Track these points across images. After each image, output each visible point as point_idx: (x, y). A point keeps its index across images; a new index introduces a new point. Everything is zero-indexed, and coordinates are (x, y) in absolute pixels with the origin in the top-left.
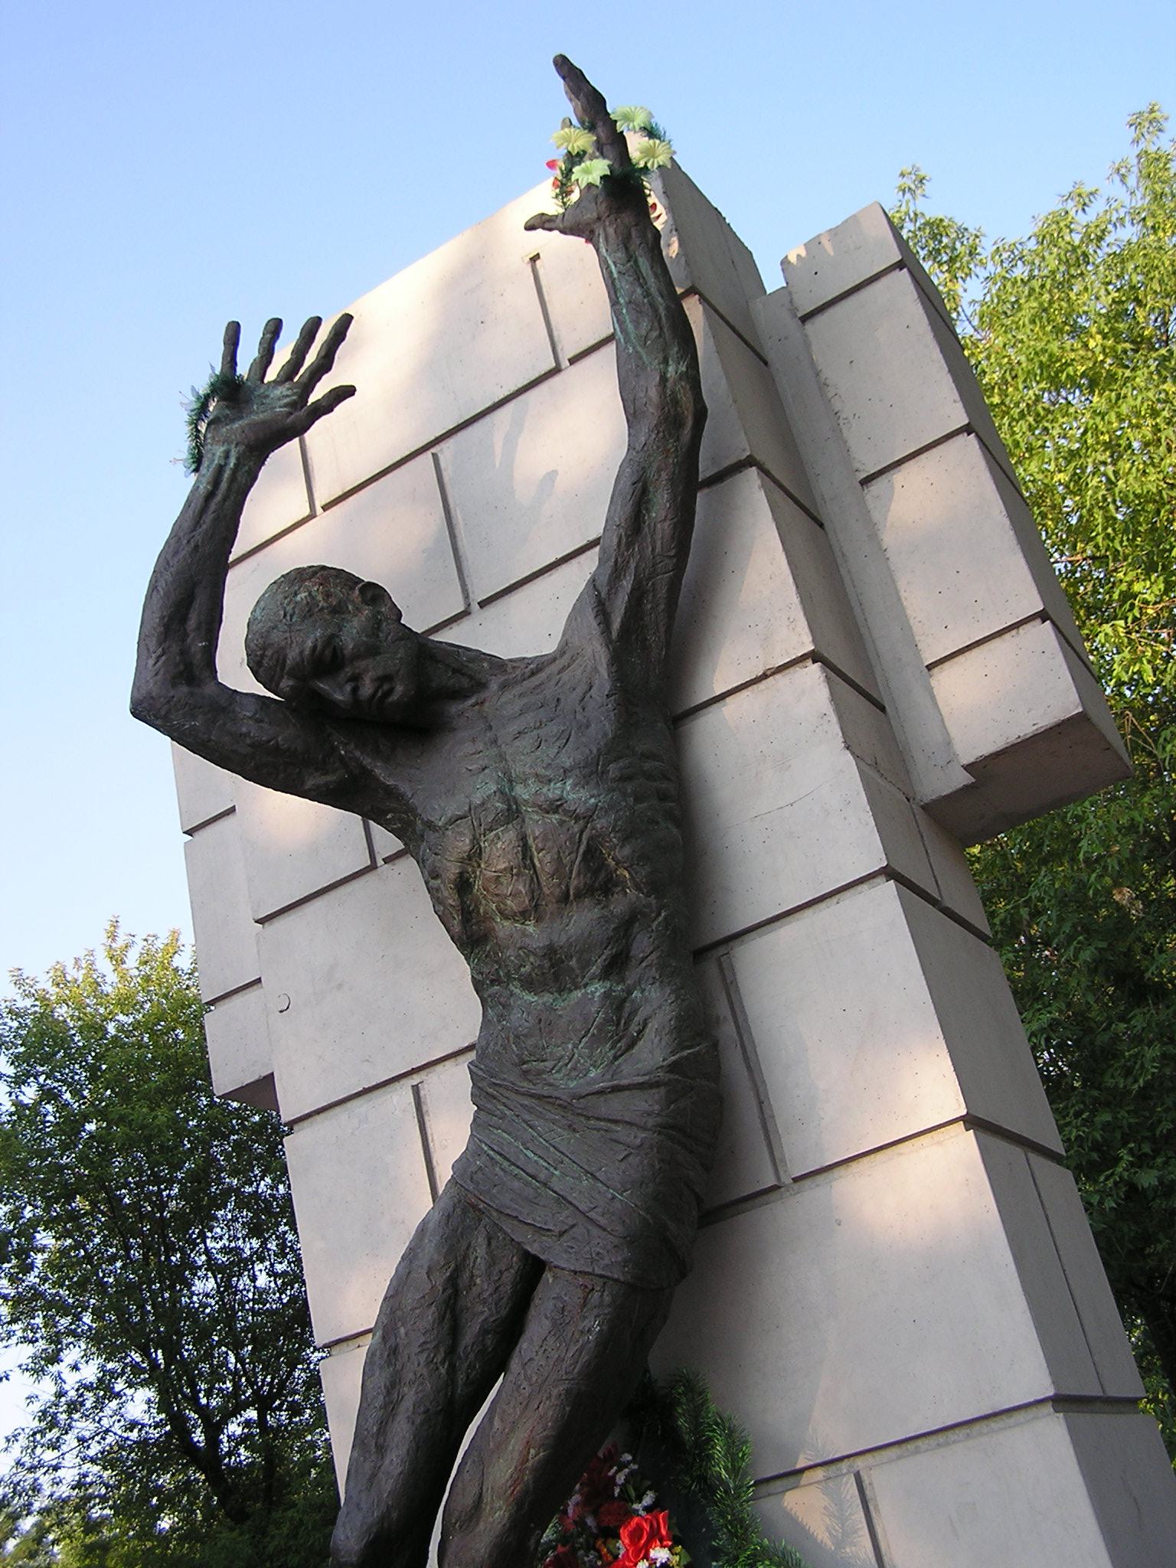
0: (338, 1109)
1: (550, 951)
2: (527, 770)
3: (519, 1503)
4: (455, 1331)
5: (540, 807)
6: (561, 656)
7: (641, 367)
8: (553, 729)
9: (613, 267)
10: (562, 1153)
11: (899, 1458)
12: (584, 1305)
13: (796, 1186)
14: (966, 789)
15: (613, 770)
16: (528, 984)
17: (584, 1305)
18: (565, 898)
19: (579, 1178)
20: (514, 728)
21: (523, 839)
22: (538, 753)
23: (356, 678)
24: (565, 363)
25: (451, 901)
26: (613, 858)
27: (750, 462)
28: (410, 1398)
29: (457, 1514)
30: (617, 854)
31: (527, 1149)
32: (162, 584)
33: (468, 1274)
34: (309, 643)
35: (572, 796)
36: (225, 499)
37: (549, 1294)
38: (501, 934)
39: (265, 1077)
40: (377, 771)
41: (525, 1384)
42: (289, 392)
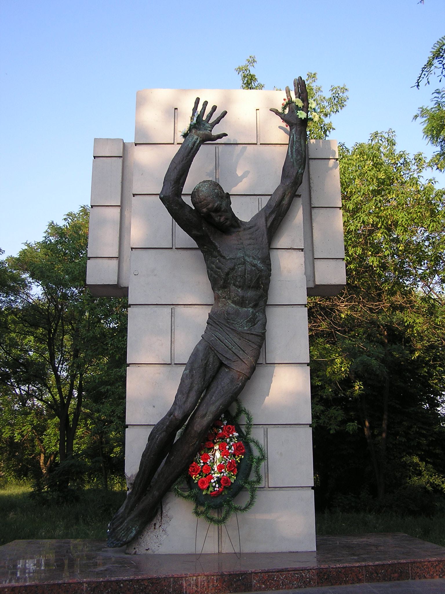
0: (146, 306)
1: (243, 297)
2: (251, 254)
4: (205, 376)
5: (252, 265)
6: (255, 226)
7: (293, 166)
9: (295, 138)
10: (236, 343)
11: (274, 427)
12: (238, 379)
13: (266, 365)
14: (311, 288)
16: (234, 302)
17: (238, 379)
18: (249, 287)
19: (240, 351)
20: (248, 242)
21: (245, 269)
22: (253, 251)
23: (221, 216)
24: (259, 143)
25: (223, 277)
26: (261, 282)
28: (196, 388)
29: (200, 415)
31: (226, 340)
32: (178, 168)
33: (208, 363)
34: (216, 204)
35: (259, 265)
36: (195, 151)
38: (232, 289)
39: (105, 285)
40: (211, 237)
41: (222, 392)
42: (210, 127)
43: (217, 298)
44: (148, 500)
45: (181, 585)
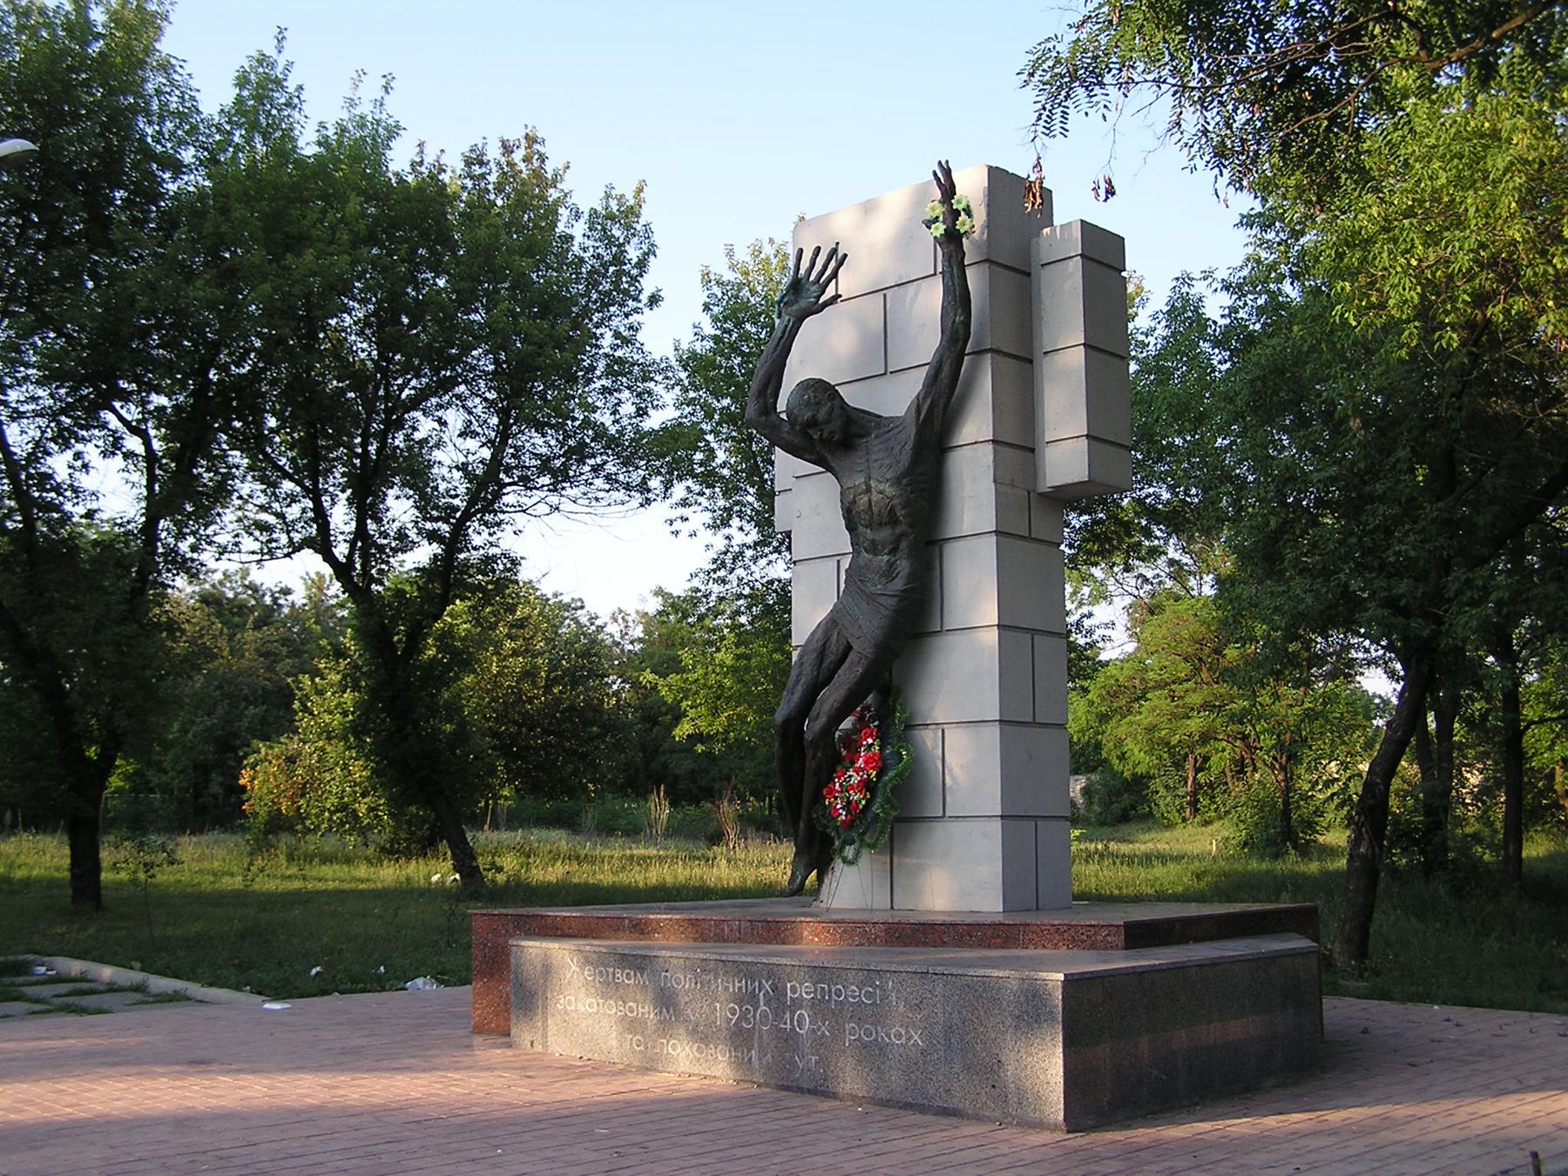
3: (830, 717)
4: (821, 662)
8: (887, 461)
15: (904, 481)
18: (880, 524)
20: (874, 457)
21: (870, 500)
23: (822, 430)
27: (991, 350)
30: (900, 513)
37: (852, 656)
45: (723, 929)
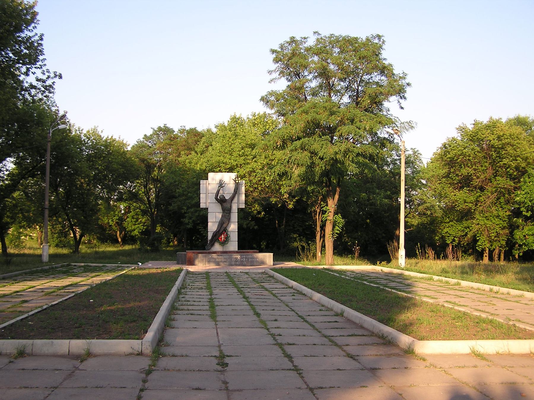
43: (223, 213)
44: (212, 243)
